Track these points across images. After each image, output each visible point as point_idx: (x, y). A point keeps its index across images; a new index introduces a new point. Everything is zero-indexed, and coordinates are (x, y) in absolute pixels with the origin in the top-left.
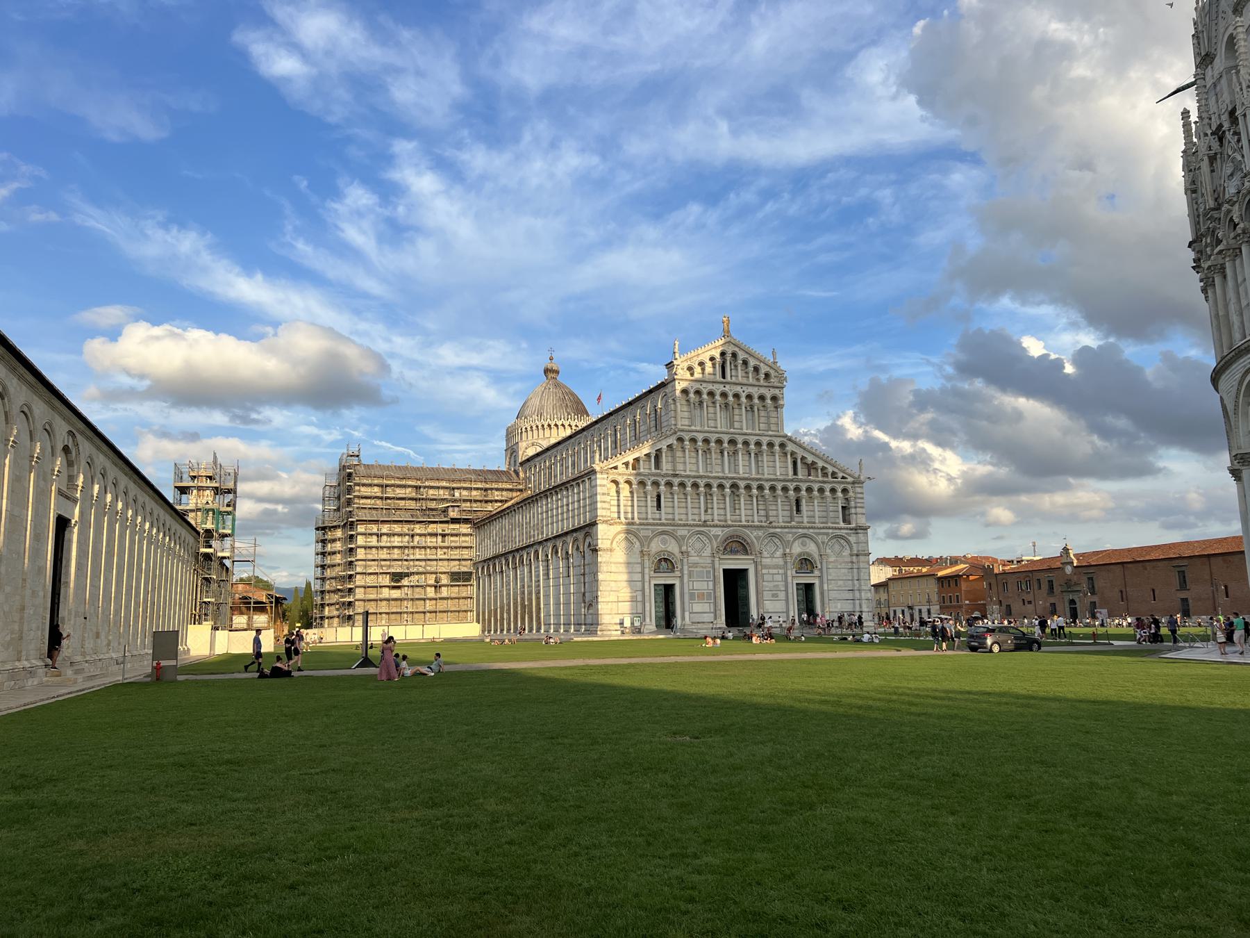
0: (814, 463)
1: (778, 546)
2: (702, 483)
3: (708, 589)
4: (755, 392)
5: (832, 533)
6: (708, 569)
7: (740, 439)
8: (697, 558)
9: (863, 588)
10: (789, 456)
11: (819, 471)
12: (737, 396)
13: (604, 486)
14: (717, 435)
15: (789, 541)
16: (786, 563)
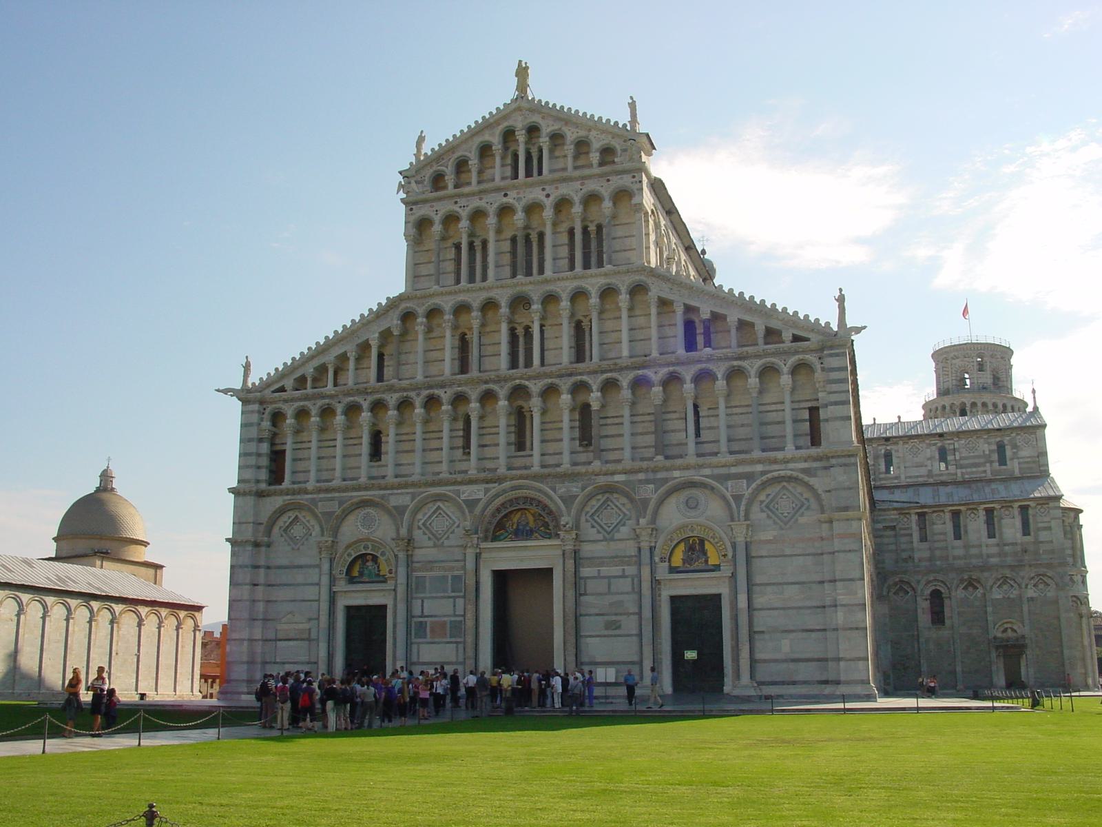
0: (716, 317)
1: (625, 514)
2: (445, 395)
3: (455, 615)
4: (574, 191)
5: (763, 473)
6: (456, 573)
7: (536, 294)
8: (434, 551)
9: (843, 599)
10: (654, 311)
11: (733, 331)
12: (532, 209)
13: (251, 425)
14: (484, 295)
15: (645, 502)
16: (639, 549)
